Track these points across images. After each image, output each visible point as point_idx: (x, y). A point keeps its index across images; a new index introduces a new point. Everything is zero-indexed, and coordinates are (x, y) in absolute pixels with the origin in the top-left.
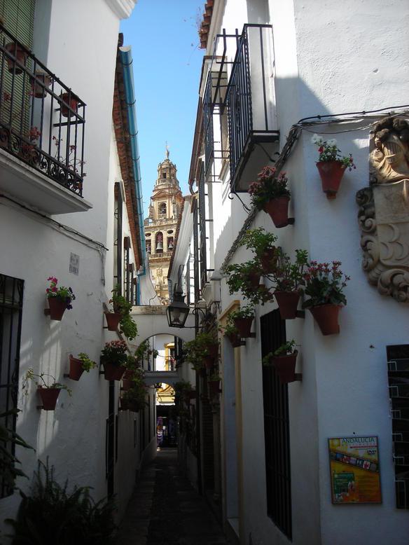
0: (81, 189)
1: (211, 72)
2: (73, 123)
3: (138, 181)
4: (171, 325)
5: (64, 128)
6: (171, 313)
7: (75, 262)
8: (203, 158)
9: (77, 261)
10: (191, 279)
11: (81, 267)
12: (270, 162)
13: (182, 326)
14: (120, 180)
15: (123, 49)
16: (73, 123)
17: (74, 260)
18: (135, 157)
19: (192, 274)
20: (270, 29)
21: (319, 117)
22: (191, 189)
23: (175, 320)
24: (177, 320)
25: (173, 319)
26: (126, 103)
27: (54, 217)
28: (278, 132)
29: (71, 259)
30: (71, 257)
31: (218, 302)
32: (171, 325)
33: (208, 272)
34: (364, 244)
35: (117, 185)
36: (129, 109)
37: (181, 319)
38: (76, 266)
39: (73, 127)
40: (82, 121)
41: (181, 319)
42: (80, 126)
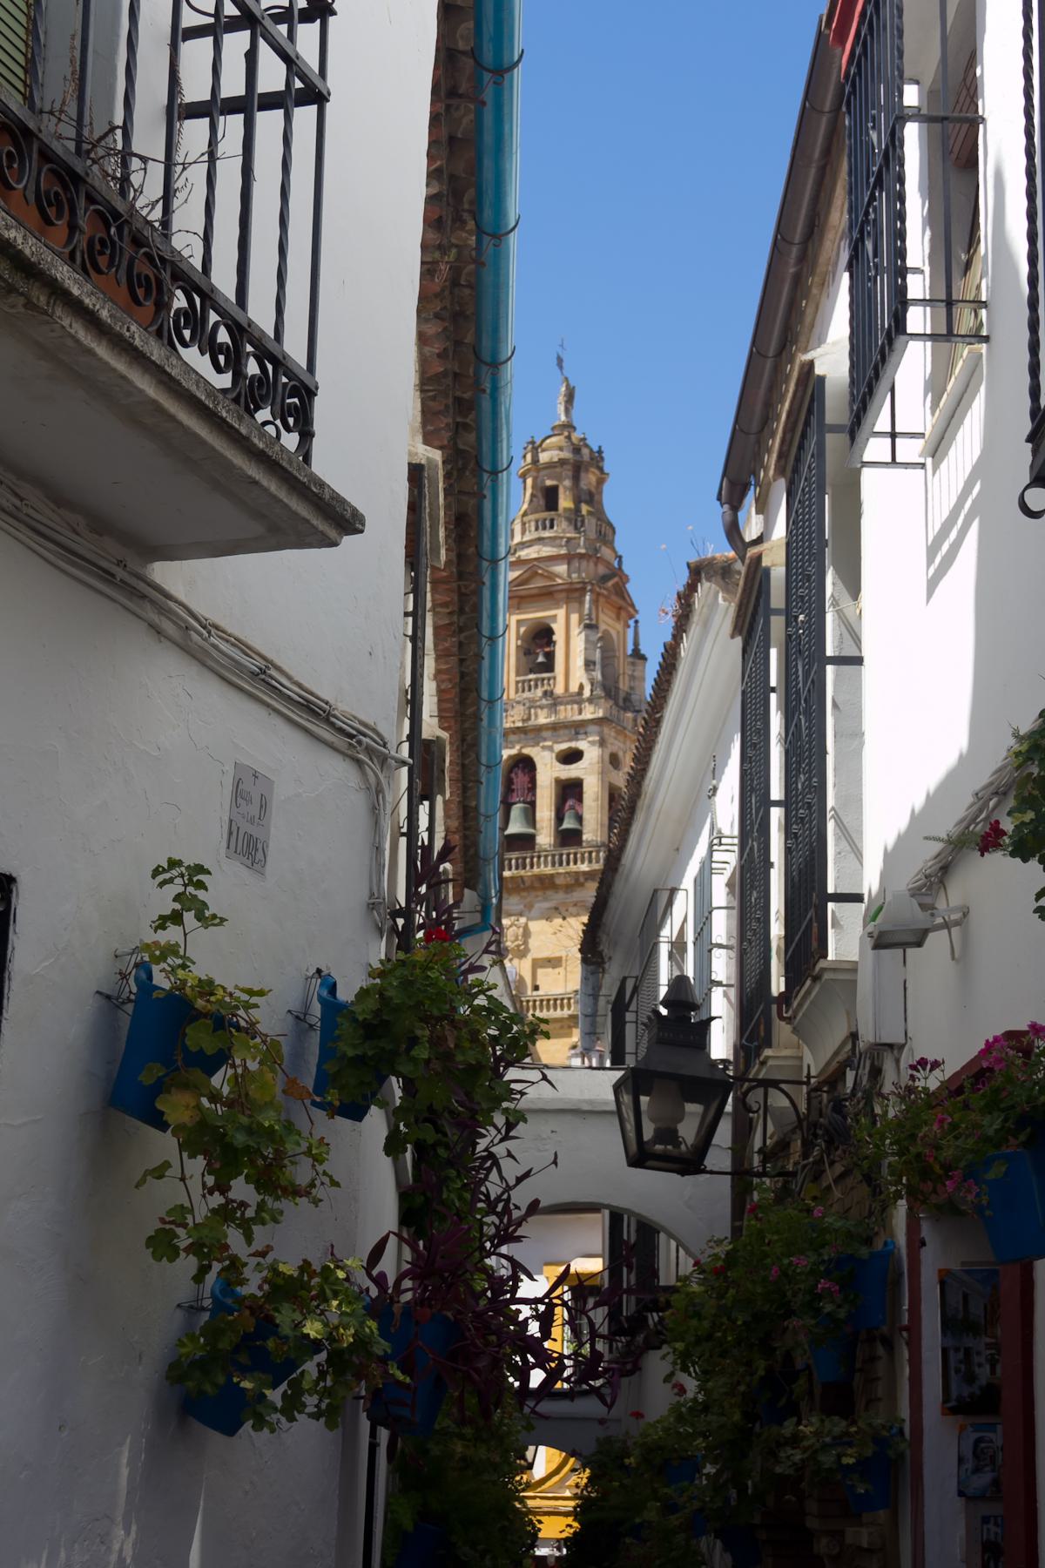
0: (307, 435)
2: (271, 101)
3: (495, 473)
4: (640, 1157)
5: (233, 125)
6: (644, 1099)
7: (254, 810)
8: (831, 355)
9: (264, 806)
10: (716, 952)
11: (279, 835)
13: (691, 1164)
16: (271, 101)
17: (249, 796)
18: (495, 351)
19: (722, 926)
22: (733, 531)
23: (660, 1136)
24: (668, 1134)
25: (648, 1132)
26: (479, 64)
27: (170, 575)
29: (238, 793)
30: (238, 783)
31: (891, 1046)
32: (640, 1157)
33: (831, 906)
35: (416, 473)
36: (488, 95)
37: (688, 1131)
39: (269, 123)
40: (315, 96)
41: (688, 1131)
42: (305, 116)
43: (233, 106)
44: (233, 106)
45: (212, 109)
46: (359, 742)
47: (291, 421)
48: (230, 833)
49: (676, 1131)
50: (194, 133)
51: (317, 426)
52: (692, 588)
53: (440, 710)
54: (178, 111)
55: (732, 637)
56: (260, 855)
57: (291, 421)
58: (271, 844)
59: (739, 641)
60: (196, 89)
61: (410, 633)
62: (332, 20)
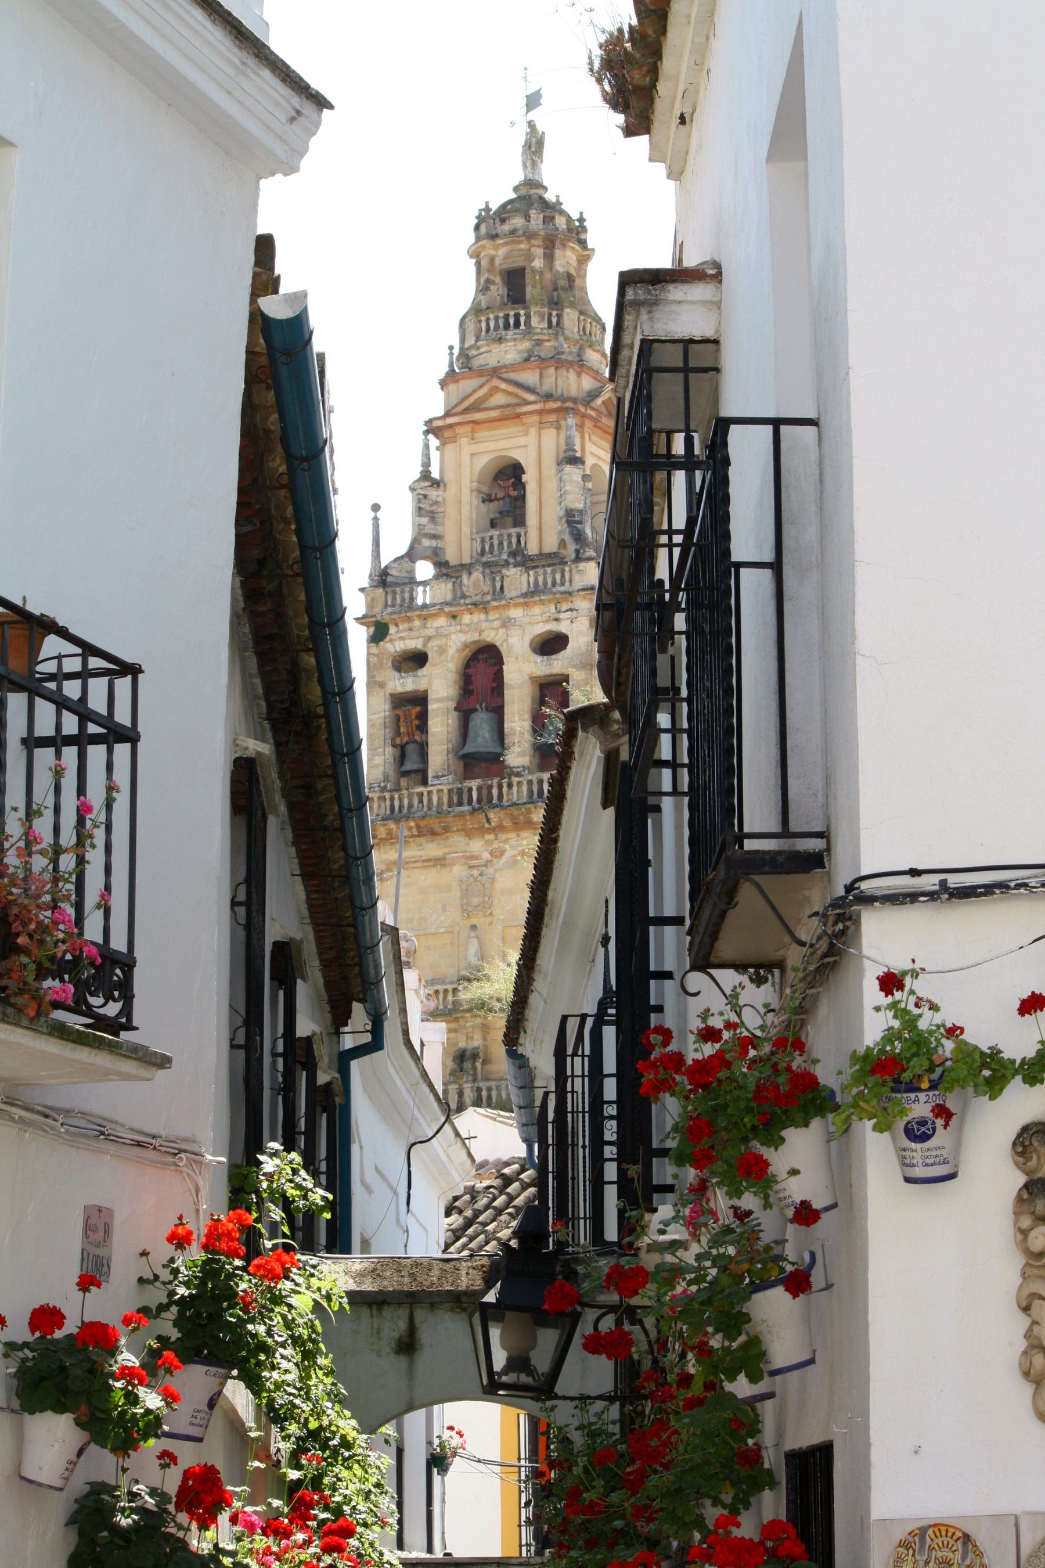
0: (128, 998)
1: (647, 345)
9: (108, 1230)
12: (795, 946)
14: (259, 747)
15: (273, 307)
16: (96, 740)
17: (97, 1225)
20: (814, 428)
21: (914, 873)
25: (500, 1359)
28: (820, 835)
29: (88, 1227)
34: (1024, 1304)
35: (244, 774)
38: (101, 1252)
39: (96, 753)
42: (122, 751)
43: (69, 741)
44: (69, 741)
45: (57, 742)
46: (181, 1159)
47: (116, 994)
48: (83, 1259)
49: (528, 1359)
50: (45, 756)
51: (136, 990)
52: (569, 736)
53: (301, 865)
54: (32, 742)
55: (605, 808)
56: (105, 1269)
57: (116, 994)
58: (114, 1258)
59: (611, 811)
60: (45, 727)
61: (243, 921)
62: (140, 676)
